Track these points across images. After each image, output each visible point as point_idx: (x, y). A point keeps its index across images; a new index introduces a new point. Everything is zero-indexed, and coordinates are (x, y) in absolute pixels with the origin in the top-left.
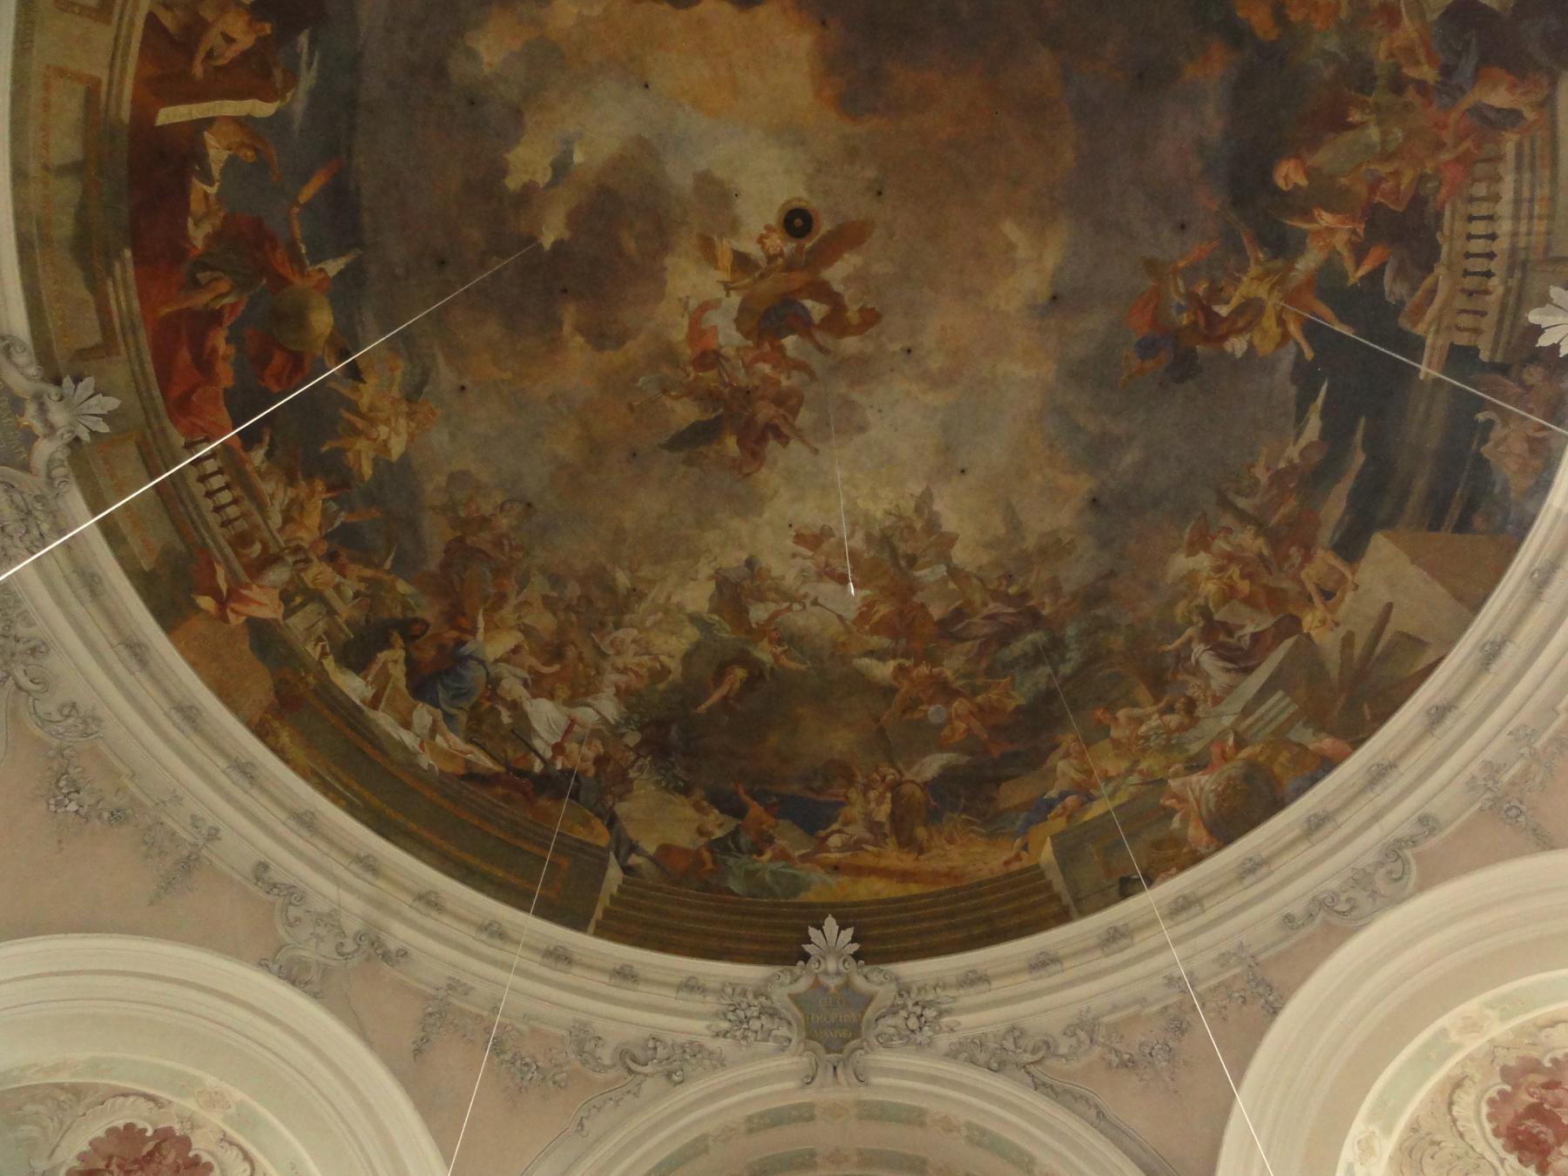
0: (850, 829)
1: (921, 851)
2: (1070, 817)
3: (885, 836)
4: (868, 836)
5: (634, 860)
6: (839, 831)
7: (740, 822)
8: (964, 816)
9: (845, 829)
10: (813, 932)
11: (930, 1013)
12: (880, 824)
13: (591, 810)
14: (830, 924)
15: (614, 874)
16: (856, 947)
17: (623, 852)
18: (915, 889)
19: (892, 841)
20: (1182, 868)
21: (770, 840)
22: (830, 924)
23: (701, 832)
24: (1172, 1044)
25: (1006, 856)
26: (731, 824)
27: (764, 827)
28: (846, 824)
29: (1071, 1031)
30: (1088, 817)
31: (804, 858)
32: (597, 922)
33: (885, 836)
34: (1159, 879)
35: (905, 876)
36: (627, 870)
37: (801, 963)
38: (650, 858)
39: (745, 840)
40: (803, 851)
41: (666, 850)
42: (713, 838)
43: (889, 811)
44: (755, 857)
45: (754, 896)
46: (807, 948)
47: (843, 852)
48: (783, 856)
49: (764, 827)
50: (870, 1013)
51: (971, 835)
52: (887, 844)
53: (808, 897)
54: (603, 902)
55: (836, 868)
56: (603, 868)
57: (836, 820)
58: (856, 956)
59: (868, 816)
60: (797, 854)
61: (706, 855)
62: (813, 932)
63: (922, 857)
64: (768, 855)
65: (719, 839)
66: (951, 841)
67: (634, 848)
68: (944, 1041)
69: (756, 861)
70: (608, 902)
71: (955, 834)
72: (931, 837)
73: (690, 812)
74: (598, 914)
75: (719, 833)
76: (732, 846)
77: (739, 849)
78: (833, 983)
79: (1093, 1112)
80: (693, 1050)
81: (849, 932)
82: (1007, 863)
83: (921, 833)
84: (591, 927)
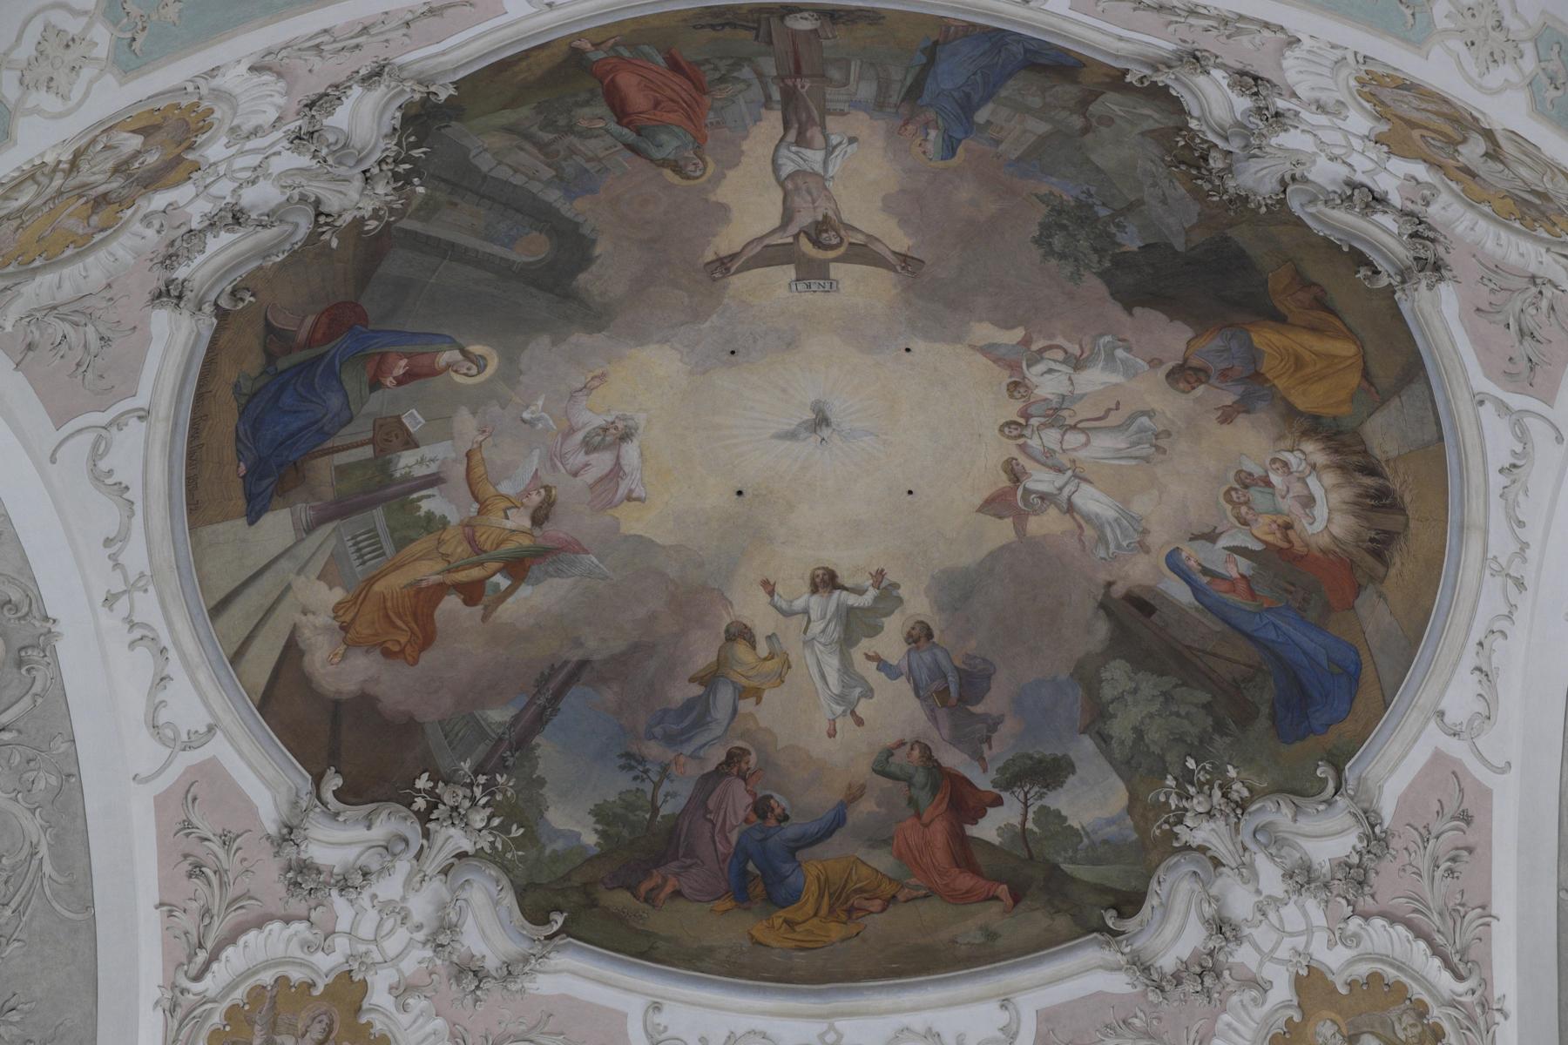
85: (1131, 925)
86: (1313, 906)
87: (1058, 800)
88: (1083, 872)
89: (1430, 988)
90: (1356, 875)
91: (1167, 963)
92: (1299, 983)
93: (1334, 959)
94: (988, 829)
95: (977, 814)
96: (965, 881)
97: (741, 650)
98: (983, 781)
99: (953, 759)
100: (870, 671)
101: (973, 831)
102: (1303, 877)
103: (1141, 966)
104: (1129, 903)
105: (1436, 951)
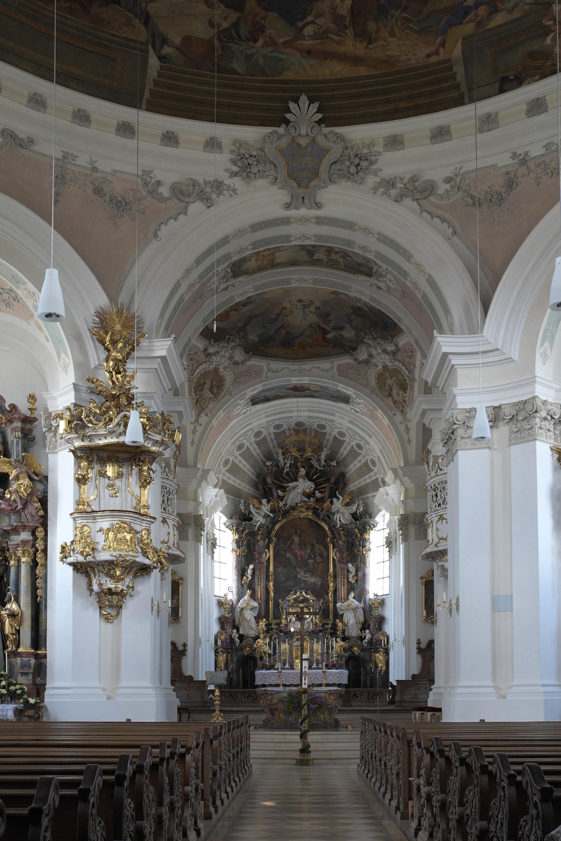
0: (319, 21)
1: (370, 41)
2: (478, 23)
3: (345, 27)
4: (333, 26)
5: (167, 50)
6: (312, 22)
7: (240, 15)
8: (404, 15)
9: (317, 21)
10: (292, 105)
11: (364, 164)
12: (342, 17)
13: (130, 11)
14: (304, 99)
15: (154, 62)
16: (320, 116)
17: (157, 44)
18: (362, 71)
19: (350, 32)
20: (544, 76)
21: (262, 29)
22: (304, 99)
23: (211, 24)
24: (504, 195)
25: (428, 50)
26: (233, 16)
27: (257, 18)
28: (318, 16)
29: (448, 180)
30: (491, 26)
31: (286, 44)
32: (147, 99)
33: (345, 27)
34: (527, 82)
35: (356, 60)
36: (162, 58)
37: (284, 125)
38: (177, 48)
39: (244, 30)
40: (286, 39)
41: (187, 39)
42: (221, 29)
43: (350, 5)
44: (251, 43)
45: (252, 75)
46: (288, 116)
47: (314, 40)
48: (272, 43)
49: (257, 18)
50: (326, 162)
51: (408, 31)
52: (346, 34)
53: (289, 75)
54: (149, 85)
55: (309, 53)
56: (146, 60)
57: (310, 14)
58: (319, 122)
59: (334, 9)
60: (282, 40)
61: (216, 43)
62: (292, 105)
63: (371, 46)
64: (261, 42)
65: (226, 29)
66: (392, 35)
67: (165, 41)
68: (371, 180)
69: (252, 47)
70: (152, 86)
71: (396, 29)
72: (378, 29)
73: (203, 8)
74: (147, 95)
75: (225, 25)
76: (235, 35)
77: (241, 39)
78: (303, 142)
79: (451, 230)
80: (218, 186)
81: (317, 105)
82: (428, 56)
83: (371, 26)
84: (144, 106)
85: (355, 353)
86: (387, 357)
87: (342, 333)
88: (346, 344)
89: (405, 373)
90: (394, 354)
91: (361, 359)
92: (383, 366)
93: (390, 364)
94: (329, 336)
95: (328, 333)
96: (325, 344)
97: (284, 311)
98: (329, 329)
99: (323, 325)
100: (308, 313)
101: (326, 336)
102: (385, 351)
103: (356, 359)
104: (354, 349)
105: (406, 369)
